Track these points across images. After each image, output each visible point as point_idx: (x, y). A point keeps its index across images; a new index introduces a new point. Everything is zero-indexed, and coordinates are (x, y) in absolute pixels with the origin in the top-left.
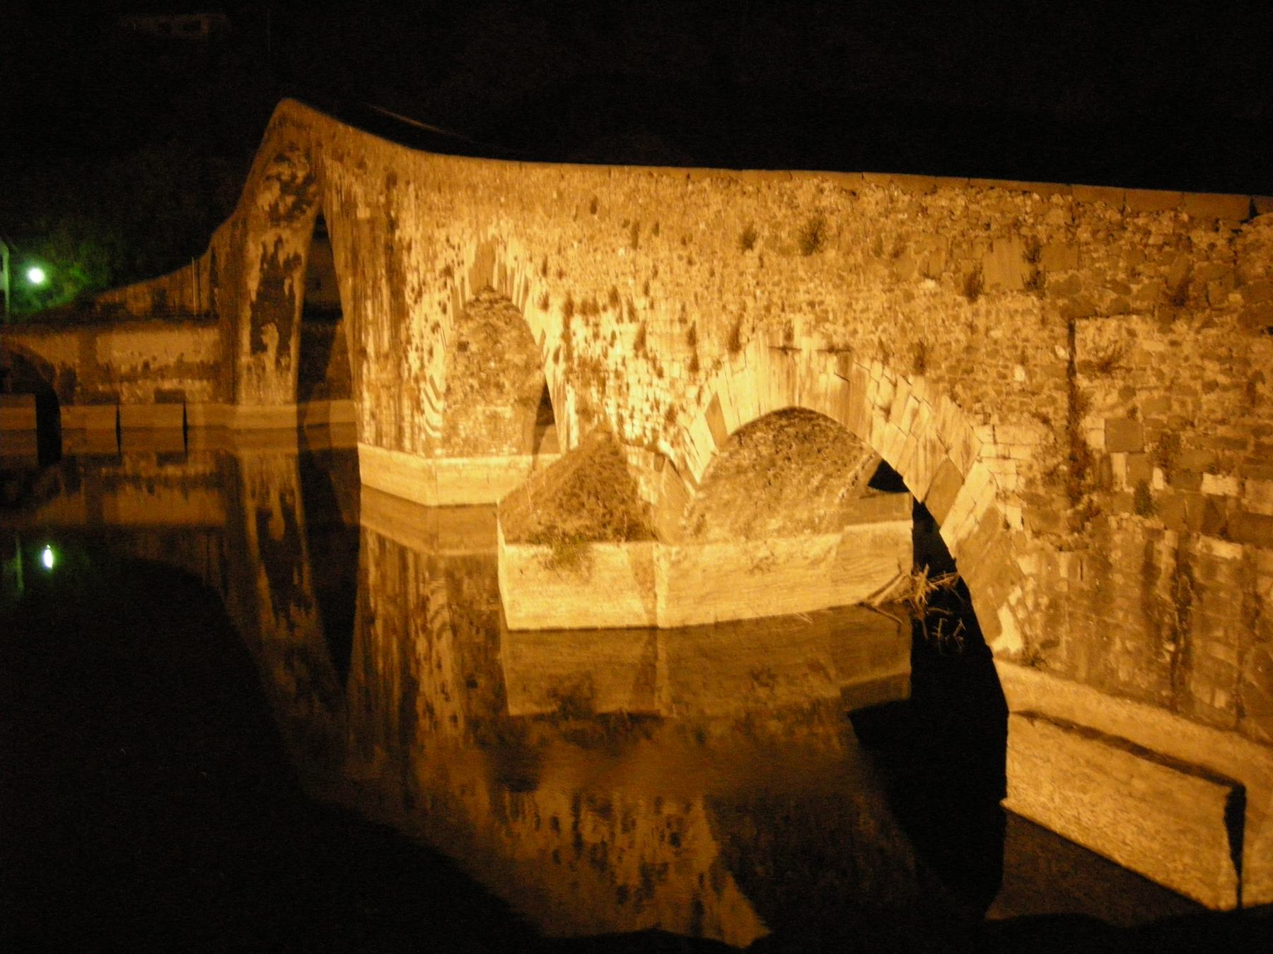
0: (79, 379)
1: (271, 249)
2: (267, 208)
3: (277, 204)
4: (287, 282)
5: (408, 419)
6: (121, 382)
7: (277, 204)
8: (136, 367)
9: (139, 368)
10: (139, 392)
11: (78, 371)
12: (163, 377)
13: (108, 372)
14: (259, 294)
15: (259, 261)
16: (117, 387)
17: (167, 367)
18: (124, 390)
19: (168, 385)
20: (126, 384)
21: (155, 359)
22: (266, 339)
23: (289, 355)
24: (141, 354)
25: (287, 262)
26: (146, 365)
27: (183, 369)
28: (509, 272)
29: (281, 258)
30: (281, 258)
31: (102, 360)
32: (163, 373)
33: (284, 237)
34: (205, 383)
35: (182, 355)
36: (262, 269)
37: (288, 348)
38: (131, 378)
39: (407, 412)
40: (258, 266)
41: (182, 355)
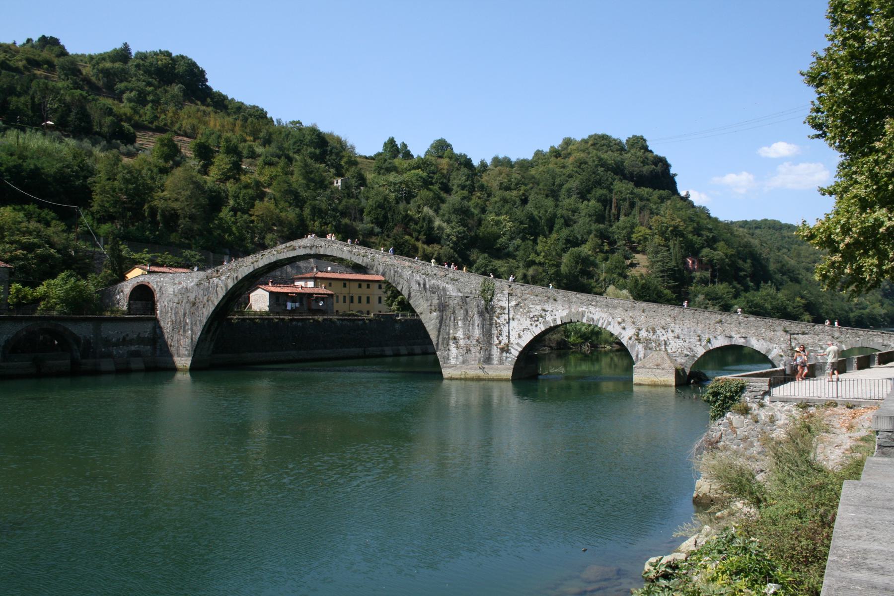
0: (92, 345)
6: (113, 347)
8: (119, 339)
9: (121, 340)
10: (121, 352)
11: (92, 341)
12: (131, 344)
13: (107, 342)
17: (133, 339)
18: (114, 351)
19: (133, 348)
20: (115, 348)
21: (127, 335)
24: (121, 333)
26: (124, 339)
27: (140, 340)
28: (595, 319)
32: (131, 342)
34: (149, 347)
35: (139, 334)
38: (117, 344)
41: (139, 334)
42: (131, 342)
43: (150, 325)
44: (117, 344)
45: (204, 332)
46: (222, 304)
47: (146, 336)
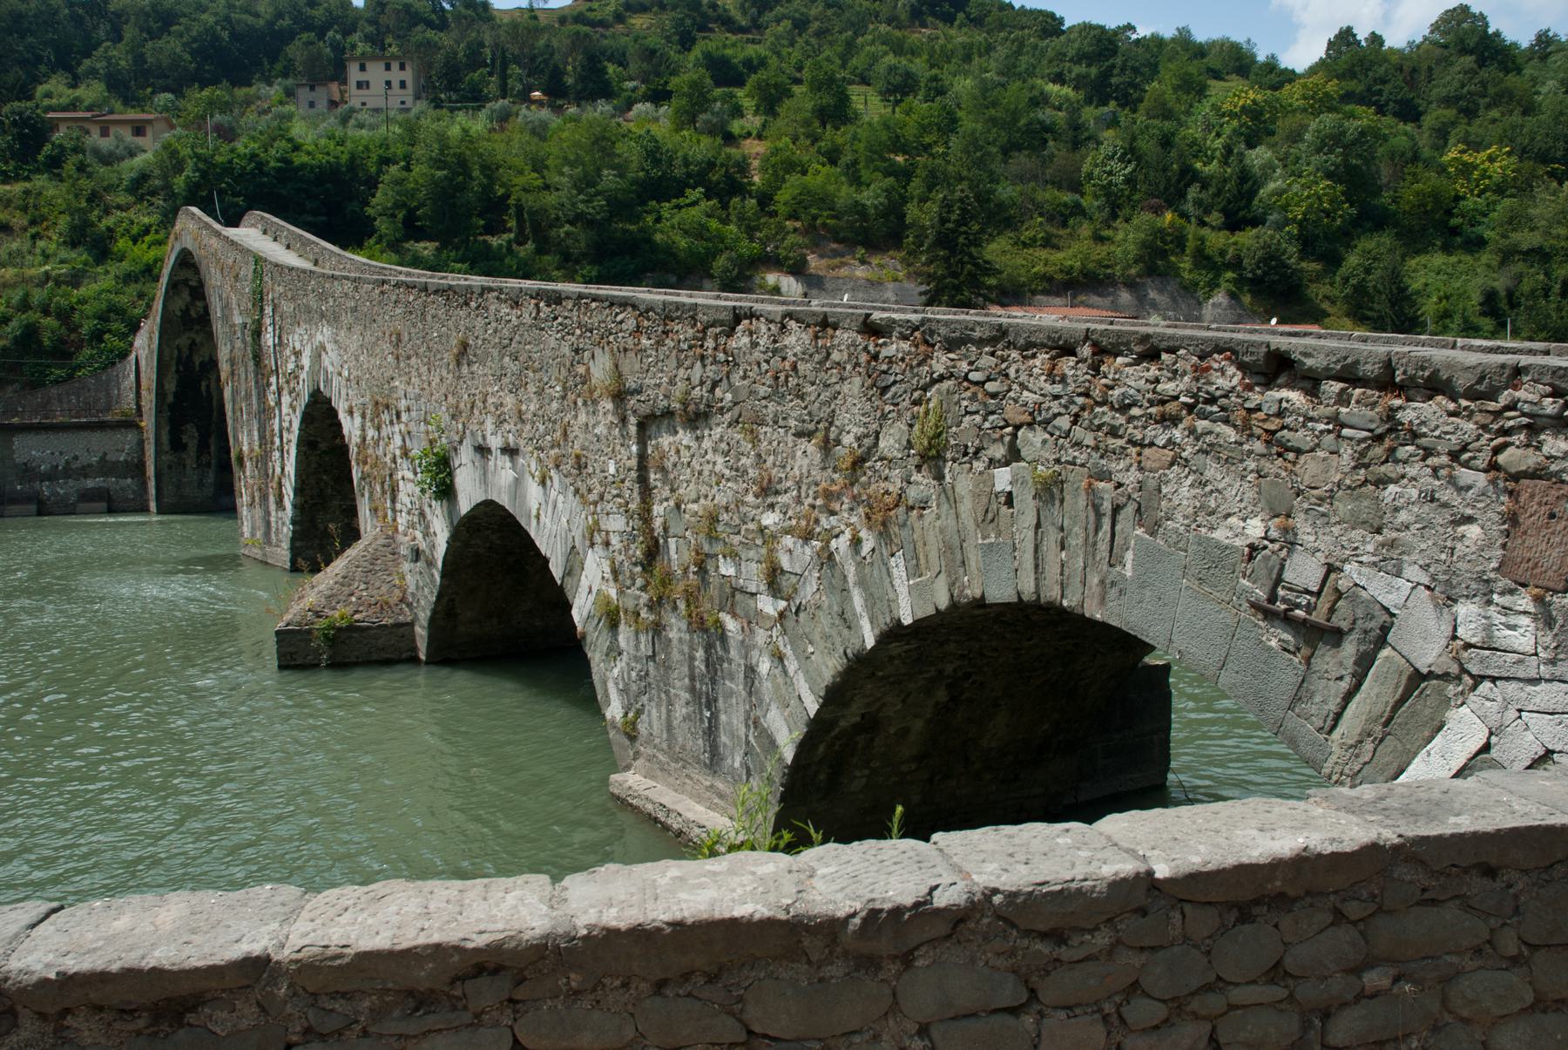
1: (186, 352)
2: (179, 313)
3: (188, 309)
4: (204, 384)
5: (273, 513)
7: (188, 309)
8: (57, 466)
10: (62, 492)
12: (86, 476)
13: (28, 472)
14: (176, 395)
15: (174, 362)
16: (37, 485)
17: (90, 466)
21: (76, 458)
22: (185, 438)
23: (209, 453)
24: (61, 453)
25: (202, 363)
29: (197, 360)
30: (197, 360)
31: (19, 458)
32: (85, 472)
33: (198, 340)
34: (129, 480)
35: (105, 454)
36: (177, 371)
37: (209, 447)
38: (51, 476)
39: (273, 507)
40: (174, 369)
41: (105, 454)
42: (85, 472)
43: (131, 436)
44: (51, 476)
45: (166, 447)
46: (171, 386)
47: (122, 459)
